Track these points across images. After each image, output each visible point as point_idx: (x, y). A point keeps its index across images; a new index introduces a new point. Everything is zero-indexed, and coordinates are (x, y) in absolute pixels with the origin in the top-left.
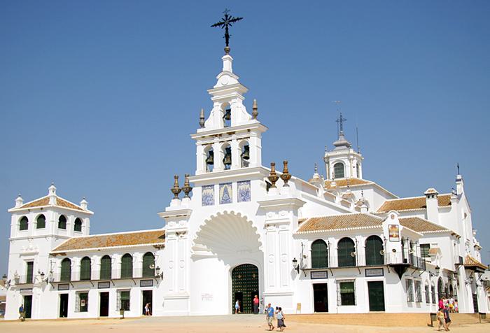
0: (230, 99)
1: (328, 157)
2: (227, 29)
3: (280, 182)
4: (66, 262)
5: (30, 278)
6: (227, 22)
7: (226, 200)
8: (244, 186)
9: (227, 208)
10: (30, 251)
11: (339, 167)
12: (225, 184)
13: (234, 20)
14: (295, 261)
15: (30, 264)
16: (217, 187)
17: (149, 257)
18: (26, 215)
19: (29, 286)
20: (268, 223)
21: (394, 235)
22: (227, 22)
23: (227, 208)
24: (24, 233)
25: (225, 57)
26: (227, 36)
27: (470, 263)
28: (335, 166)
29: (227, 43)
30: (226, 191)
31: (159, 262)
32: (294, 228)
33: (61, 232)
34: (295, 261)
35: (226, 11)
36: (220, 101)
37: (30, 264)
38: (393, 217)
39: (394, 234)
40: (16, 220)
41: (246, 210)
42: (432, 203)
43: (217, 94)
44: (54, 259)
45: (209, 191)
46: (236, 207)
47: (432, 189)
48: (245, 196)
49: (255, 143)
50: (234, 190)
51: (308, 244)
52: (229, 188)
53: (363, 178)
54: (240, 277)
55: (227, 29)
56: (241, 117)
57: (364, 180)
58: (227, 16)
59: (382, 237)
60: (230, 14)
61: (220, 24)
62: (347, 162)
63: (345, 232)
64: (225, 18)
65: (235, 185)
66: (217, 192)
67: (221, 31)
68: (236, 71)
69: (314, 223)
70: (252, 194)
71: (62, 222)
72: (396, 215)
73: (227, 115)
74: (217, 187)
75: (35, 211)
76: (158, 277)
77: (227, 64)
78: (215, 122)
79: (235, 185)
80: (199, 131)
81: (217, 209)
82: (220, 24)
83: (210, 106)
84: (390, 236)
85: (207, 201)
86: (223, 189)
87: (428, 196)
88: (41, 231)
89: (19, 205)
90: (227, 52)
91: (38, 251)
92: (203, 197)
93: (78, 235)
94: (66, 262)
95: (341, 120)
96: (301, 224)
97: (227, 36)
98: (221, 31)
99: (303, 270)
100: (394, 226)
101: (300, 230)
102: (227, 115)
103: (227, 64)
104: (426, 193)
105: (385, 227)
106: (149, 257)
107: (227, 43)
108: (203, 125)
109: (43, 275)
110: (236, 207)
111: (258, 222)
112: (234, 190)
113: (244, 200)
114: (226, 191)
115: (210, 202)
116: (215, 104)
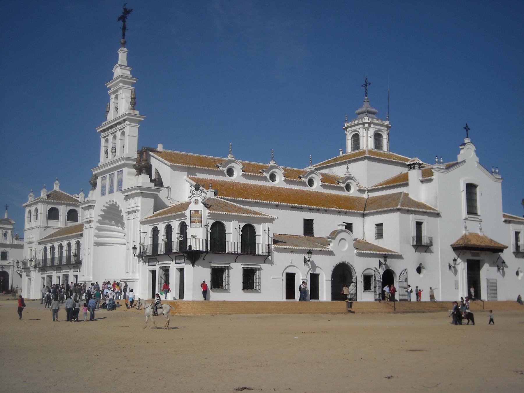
1: (346, 128)
7: (111, 191)
8: (119, 177)
14: (135, 248)
21: (197, 221)
26: (124, 29)
29: (124, 35)
34: (135, 248)
35: (125, 5)
39: (196, 219)
41: (118, 198)
45: (104, 181)
53: (390, 148)
55: (124, 22)
58: (125, 9)
62: (362, 132)
67: (121, 23)
68: (131, 62)
77: (122, 56)
84: (191, 222)
90: (124, 44)
97: (124, 29)
100: (196, 212)
103: (122, 56)
105: (187, 213)
107: (124, 35)
114: (112, 182)
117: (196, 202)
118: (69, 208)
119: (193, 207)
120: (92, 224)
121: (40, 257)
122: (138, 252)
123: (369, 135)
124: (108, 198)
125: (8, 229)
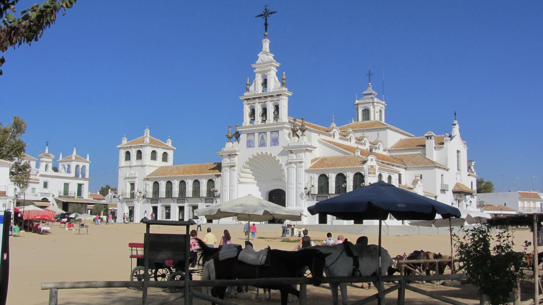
0: (267, 71)
1: (358, 104)
2: (266, 19)
3: (299, 133)
4: (156, 185)
5: (133, 195)
6: (266, 14)
9: (264, 150)
10: (131, 176)
11: (366, 112)
12: (262, 133)
13: (271, 13)
14: (306, 188)
15: (133, 185)
16: (257, 135)
17: (211, 182)
18: (129, 150)
19: (132, 200)
20: (289, 161)
22: (266, 14)
23: (264, 150)
24: (128, 163)
25: (264, 40)
26: (266, 25)
27: (458, 189)
28: (363, 111)
30: (262, 138)
31: (217, 187)
32: (308, 165)
33: (153, 163)
35: (266, 6)
36: (260, 72)
37: (133, 185)
38: (372, 160)
40: (122, 153)
42: (430, 144)
43: (258, 68)
44: (148, 182)
45: (251, 137)
46: (269, 150)
47: (430, 132)
48: (275, 142)
49: (284, 104)
50: (268, 137)
51: (316, 177)
52: (265, 136)
54: (274, 198)
55: (266, 19)
56: (274, 84)
57: (385, 124)
58: (266, 10)
59: (363, 173)
60: (268, 8)
61: (261, 15)
62: (372, 109)
63: (340, 169)
64: (265, 11)
65: (268, 133)
66: (257, 138)
67: (262, 20)
69: (322, 162)
70: (280, 141)
71: (154, 155)
72: (374, 159)
73: (265, 83)
74: (257, 135)
75: (135, 147)
76: (217, 197)
77: (266, 45)
78: (257, 88)
79: (268, 133)
80: (246, 94)
81: (257, 150)
82: (261, 15)
83: (253, 77)
84: (369, 173)
85: (250, 144)
86: (260, 136)
87: (427, 137)
88: (139, 162)
89: (125, 142)
91: (137, 175)
92: (247, 141)
93: (164, 164)
94: (156, 185)
95: (370, 75)
96: (313, 163)
97: (266, 25)
98: (262, 20)
99: (312, 195)
100: (372, 166)
101: (311, 167)
102: (265, 83)
103: (266, 45)
104: (426, 135)
105: (365, 166)
106: (211, 182)
108: (248, 90)
109: (140, 192)
110: (269, 150)
111: (283, 160)
112: (268, 137)
113: (275, 145)
114: (262, 138)
115: (252, 145)
116: (257, 75)
117: (372, 160)
118: (126, 150)
119: (369, 163)
120: (236, 168)
121: (150, 189)
122: (308, 190)
123: (376, 110)
124: (257, 150)
125: (49, 162)
